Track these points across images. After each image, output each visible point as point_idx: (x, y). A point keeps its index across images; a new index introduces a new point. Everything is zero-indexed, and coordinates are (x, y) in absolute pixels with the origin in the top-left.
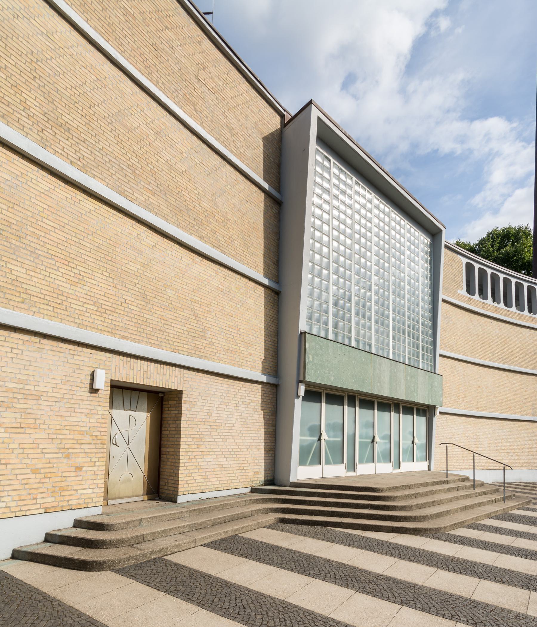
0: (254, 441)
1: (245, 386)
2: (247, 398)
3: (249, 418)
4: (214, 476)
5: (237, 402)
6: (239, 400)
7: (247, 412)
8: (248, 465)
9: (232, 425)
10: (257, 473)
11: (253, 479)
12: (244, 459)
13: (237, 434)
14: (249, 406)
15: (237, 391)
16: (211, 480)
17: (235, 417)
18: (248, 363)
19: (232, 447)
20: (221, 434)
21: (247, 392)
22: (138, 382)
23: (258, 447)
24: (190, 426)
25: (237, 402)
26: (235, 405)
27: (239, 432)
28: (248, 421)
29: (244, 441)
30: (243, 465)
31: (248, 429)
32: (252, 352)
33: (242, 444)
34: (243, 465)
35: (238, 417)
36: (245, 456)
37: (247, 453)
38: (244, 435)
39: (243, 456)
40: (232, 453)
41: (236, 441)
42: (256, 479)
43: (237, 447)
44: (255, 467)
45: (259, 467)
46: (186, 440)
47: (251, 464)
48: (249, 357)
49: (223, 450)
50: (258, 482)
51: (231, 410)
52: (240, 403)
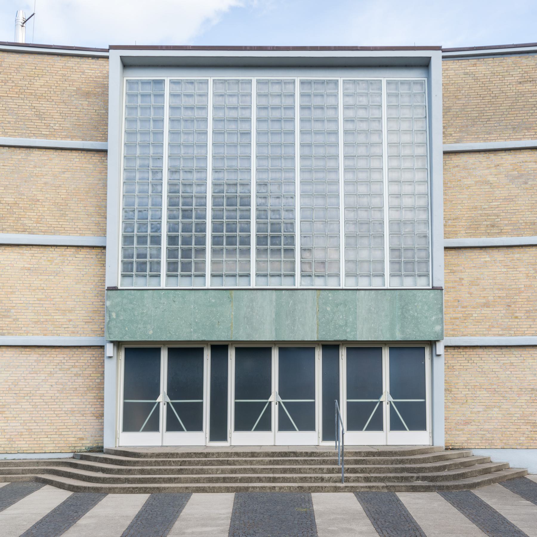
0: (77, 406)
1: (62, 353)
4: (22, 439)
6: (55, 367)
7: (66, 378)
8: (68, 430)
9: (46, 392)
10: (82, 439)
11: (76, 445)
13: (53, 401)
14: (68, 372)
15: (51, 358)
16: (17, 442)
18: (66, 329)
19: (45, 412)
21: (66, 358)
23: (82, 412)
25: (52, 370)
26: (49, 372)
30: (60, 430)
31: (68, 395)
32: (71, 318)
33: (58, 409)
34: (60, 430)
36: (63, 421)
38: (62, 401)
39: (60, 421)
40: (44, 418)
41: (50, 406)
42: (80, 445)
43: (52, 412)
44: (78, 433)
47: (71, 430)
48: (68, 323)
50: (84, 448)
51: (44, 378)
52: (57, 370)
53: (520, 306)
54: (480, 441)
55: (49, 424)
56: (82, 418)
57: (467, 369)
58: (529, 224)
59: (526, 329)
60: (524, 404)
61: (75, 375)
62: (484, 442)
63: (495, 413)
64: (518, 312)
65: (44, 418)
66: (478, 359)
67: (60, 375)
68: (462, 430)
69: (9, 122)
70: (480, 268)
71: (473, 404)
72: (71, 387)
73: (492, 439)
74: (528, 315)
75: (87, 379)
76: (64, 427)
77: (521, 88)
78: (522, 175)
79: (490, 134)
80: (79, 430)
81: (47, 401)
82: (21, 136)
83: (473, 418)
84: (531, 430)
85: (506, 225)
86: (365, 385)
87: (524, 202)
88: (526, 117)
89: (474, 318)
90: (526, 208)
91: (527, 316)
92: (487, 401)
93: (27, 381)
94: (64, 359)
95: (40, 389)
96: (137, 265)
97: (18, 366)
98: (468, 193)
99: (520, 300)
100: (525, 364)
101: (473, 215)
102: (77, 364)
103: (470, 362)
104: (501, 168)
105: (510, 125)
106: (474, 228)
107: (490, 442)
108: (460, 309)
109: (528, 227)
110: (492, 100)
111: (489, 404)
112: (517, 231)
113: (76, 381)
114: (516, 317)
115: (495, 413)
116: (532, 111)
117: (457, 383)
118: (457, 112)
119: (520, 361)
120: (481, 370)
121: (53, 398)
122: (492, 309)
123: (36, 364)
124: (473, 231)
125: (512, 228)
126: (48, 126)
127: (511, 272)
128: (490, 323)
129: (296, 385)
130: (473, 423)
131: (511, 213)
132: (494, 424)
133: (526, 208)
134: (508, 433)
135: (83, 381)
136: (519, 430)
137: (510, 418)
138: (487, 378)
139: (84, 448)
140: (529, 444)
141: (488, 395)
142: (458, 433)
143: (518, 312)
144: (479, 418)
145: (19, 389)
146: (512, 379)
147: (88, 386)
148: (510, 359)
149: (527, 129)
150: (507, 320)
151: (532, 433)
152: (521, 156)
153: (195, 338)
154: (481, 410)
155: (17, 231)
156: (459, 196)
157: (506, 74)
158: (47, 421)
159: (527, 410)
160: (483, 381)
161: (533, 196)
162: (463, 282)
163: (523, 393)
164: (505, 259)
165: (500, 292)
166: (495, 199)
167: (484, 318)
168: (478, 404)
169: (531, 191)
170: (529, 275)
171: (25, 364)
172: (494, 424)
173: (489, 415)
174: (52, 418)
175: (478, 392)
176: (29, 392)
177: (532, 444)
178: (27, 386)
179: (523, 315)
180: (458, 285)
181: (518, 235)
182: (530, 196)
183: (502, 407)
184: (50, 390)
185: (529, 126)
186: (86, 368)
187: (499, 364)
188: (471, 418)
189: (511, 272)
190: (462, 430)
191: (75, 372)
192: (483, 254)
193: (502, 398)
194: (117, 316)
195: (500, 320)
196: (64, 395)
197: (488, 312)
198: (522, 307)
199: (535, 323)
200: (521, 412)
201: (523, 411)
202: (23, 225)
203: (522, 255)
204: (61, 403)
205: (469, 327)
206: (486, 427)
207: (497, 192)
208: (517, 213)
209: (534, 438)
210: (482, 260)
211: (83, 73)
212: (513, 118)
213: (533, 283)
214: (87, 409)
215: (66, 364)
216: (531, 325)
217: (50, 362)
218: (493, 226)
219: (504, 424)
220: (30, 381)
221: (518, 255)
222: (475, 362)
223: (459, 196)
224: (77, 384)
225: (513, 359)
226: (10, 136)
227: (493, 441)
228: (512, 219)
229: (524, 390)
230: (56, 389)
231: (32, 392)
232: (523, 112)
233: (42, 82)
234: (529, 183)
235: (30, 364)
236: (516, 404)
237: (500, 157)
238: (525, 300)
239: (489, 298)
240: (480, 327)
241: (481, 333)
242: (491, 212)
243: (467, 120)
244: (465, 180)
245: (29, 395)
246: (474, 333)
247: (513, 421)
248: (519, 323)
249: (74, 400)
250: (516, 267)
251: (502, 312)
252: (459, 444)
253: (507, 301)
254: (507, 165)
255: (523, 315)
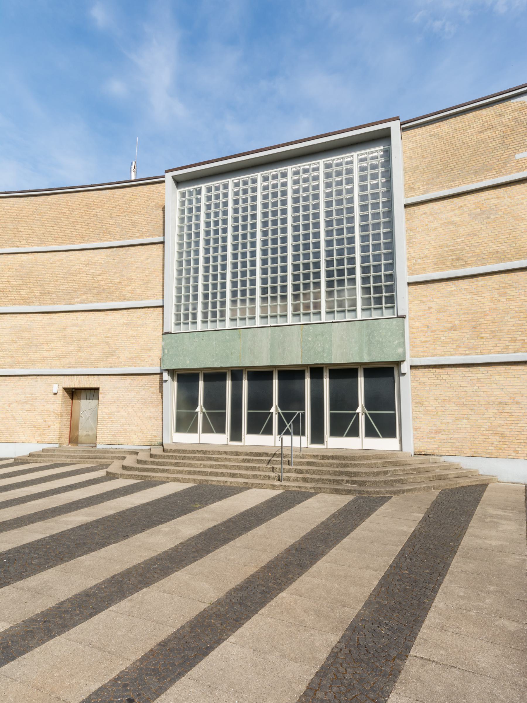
53: (485, 327)
54: (450, 449)
57: (436, 385)
58: (492, 254)
59: (492, 348)
60: (492, 416)
62: (454, 449)
63: (463, 423)
64: (483, 333)
66: (447, 376)
68: (434, 438)
69: (117, 232)
70: (446, 297)
71: (443, 416)
73: (461, 447)
74: (494, 335)
77: (482, 136)
78: (485, 211)
79: (453, 181)
82: (124, 239)
83: (444, 428)
84: (500, 440)
85: (470, 257)
86: (344, 401)
87: (487, 235)
88: (487, 160)
89: (442, 340)
90: (489, 239)
91: (493, 336)
92: (456, 413)
96: (186, 316)
98: (435, 235)
99: (486, 322)
100: (491, 380)
101: (440, 252)
103: (439, 378)
104: (464, 208)
105: (472, 170)
106: (440, 263)
107: (460, 450)
108: (429, 333)
109: (491, 256)
110: (455, 152)
111: (458, 416)
112: (482, 261)
114: (482, 338)
115: (463, 423)
116: (492, 154)
117: (428, 397)
118: (423, 169)
119: (487, 377)
120: (449, 386)
122: (458, 332)
124: (440, 266)
125: (475, 259)
126: (139, 231)
127: (476, 298)
128: (457, 345)
129: (291, 400)
130: (443, 433)
131: (475, 246)
132: (463, 434)
133: (489, 239)
134: (477, 442)
136: (487, 440)
137: (478, 429)
138: (456, 393)
140: (498, 454)
141: (457, 408)
142: (429, 441)
143: (483, 333)
144: (449, 428)
146: (480, 393)
148: (477, 375)
149: (489, 170)
150: (474, 341)
151: (501, 443)
152: (483, 195)
153: (216, 365)
154: (450, 421)
155: (120, 300)
156: (427, 238)
157: (467, 127)
159: (495, 421)
160: (452, 396)
161: (496, 228)
162: (432, 310)
163: (490, 406)
164: (470, 287)
165: (466, 316)
166: (460, 236)
167: (451, 340)
168: (448, 416)
169: (493, 224)
170: (494, 299)
172: (463, 434)
173: (458, 426)
175: (448, 405)
177: (501, 454)
179: (488, 335)
180: (427, 313)
181: (482, 265)
182: (492, 229)
183: (471, 418)
185: (490, 167)
187: (466, 380)
188: (441, 428)
189: (476, 298)
190: (434, 438)
192: (450, 284)
193: (470, 411)
194: (168, 352)
195: (467, 341)
197: (455, 335)
198: (487, 328)
199: (500, 342)
200: (489, 424)
201: (491, 423)
202: (124, 296)
203: (485, 282)
205: (438, 348)
206: (455, 436)
207: (461, 230)
208: (481, 246)
209: (503, 449)
210: (448, 289)
211: (160, 192)
212: (474, 164)
213: (497, 306)
216: (496, 344)
218: (458, 260)
219: (473, 434)
221: (482, 283)
222: (444, 378)
223: (427, 238)
225: (480, 376)
226: (118, 240)
227: (462, 449)
228: (476, 251)
229: (491, 403)
232: (484, 156)
233: (136, 203)
234: (492, 217)
236: (484, 416)
237: (463, 199)
238: (491, 322)
239: (456, 322)
240: (448, 348)
241: (449, 353)
242: (456, 247)
243: (433, 173)
244: (432, 224)
246: (443, 353)
247: (481, 432)
248: (485, 343)
250: (480, 293)
251: (468, 334)
252: (430, 451)
253: (473, 323)
254: (469, 205)
255: (488, 335)
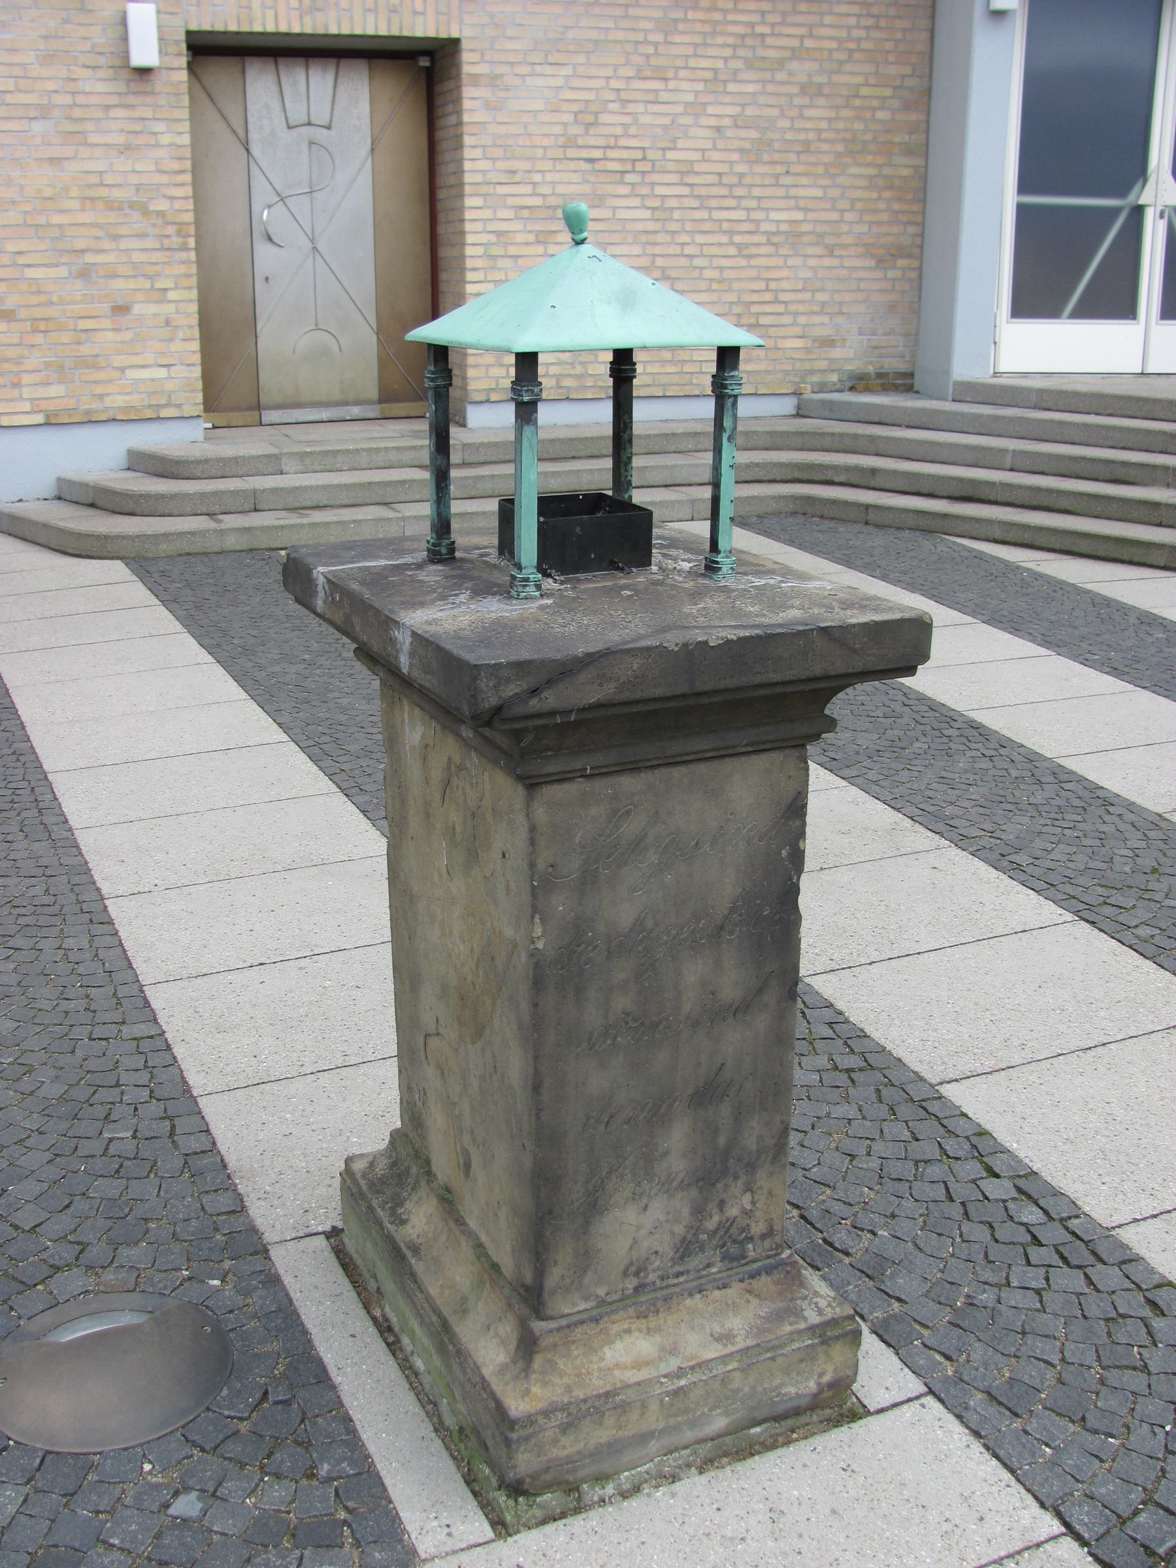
0: (811, 216)
2: (769, 41)
3: (785, 123)
5: (720, 64)
6: (728, 52)
8: (780, 308)
9: (696, 156)
10: (828, 342)
11: (807, 366)
12: (761, 285)
14: (780, 76)
15: (717, 16)
17: (713, 122)
19: (699, 239)
20: (645, 191)
22: (283, 28)
23: (829, 240)
24: (502, 165)
25: (720, 64)
26: (709, 75)
27: (735, 180)
28: (776, 136)
29: (760, 215)
30: (755, 309)
31: (779, 169)
33: (746, 227)
34: (755, 309)
35: (727, 122)
36: (765, 275)
37: (773, 262)
38: (756, 192)
39: (754, 273)
40: (697, 262)
41: (716, 215)
42: (823, 365)
44: (817, 319)
45: (840, 320)
46: (487, 214)
49: (658, 250)
51: (690, 98)
55: (715, 286)
56: (827, 262)
61: (804, 89)
65: (697, 262)
67: (750, 88)
72: (789, 136)
75: (847, 106)
76: (768, 297)
80: (816, 308)
81: (703, 191)
93: (632, 108)
94: (763, 23)
95: (680, 144)
97: (596, 42)
102: (809, 43)
113: (808, 113)
121: (725, 180)
123: (658, 37)
135: (832, 114)
139: (834, 378)
145: (601, 142)
147: (848, 136)
158: (708, 274)
171: (620, 36)
174: (725, 263)
176: (638, 155)
178: (632, 131)
184: (715, 148)
186: (841, 63)
191: (804, 79)
196: (766, 169)
204: (753, 204)
214: (845, 228)
215: (769, 41)
217: (714, 33)
220: (640, 108)
224: (809, 125)
230: (736, 144)
231: (651, 155)
235: (641, 38)
245: (640, 167)
249: (801, 192)
